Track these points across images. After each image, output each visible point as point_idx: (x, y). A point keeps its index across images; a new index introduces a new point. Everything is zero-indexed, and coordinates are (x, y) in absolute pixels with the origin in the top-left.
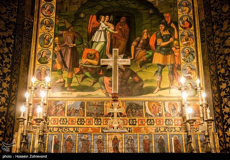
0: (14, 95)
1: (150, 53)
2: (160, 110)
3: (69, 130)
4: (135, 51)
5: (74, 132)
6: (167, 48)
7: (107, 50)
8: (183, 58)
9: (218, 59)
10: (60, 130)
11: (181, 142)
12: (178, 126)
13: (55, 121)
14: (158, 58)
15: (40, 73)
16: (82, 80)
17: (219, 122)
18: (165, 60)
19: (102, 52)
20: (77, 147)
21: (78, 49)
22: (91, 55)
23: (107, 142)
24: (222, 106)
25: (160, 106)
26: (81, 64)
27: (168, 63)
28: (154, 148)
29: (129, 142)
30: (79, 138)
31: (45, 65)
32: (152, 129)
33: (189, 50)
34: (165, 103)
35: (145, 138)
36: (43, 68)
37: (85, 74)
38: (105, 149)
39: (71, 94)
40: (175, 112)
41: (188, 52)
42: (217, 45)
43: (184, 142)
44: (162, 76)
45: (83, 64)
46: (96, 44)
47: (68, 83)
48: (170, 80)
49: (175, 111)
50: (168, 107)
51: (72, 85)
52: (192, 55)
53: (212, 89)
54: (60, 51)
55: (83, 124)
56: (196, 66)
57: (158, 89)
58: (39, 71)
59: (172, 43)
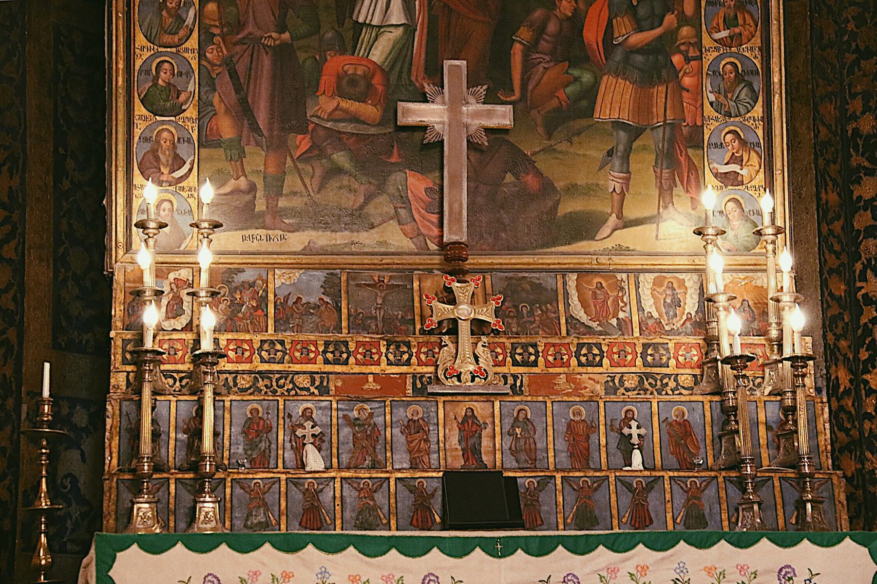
1: (587, 77)
2: (621, 304)
3: (294, 384)
4: (528, 67)
5: (312, 389)
6: (651, 57)
7: (415, 61)
8: (712, 98)
9: (851, 72)
11: (698, 431)
13: (240, 351)
14: (615, 100)
15: (154, 152)
16: (321, 187)
17: (838, 339)
18: (642, 106)
19: (397, 68)
20: (335, 445)
21: (302, 56)
22: (353, 82)
23: (441, 428)
25: (622, 289)
26: (317, 117)
27: (653, 119)
28: (604, 449)
29: (518, 431)
30: (341, 414)
31: (173, 118)
32: (593, 380)
33: (739, 66)
34: (642, 277)
35: (574, 415)
36: (165, 134)
38: (435, 452)
40: (676, 316)
41: (732, 75)
42: (853, 11)
43: (708, 429)
44: (628, 172)
45: (323, 119)
46: (373, 35)
48: (661, 188)
49: (678, 311)
51: (282, 203)
52: (750, 85)
54: (228, 63)
55: (346, 363)
56: (760, 132)
57: (613, 220)
58: (147, 147)
59: (671, 35)
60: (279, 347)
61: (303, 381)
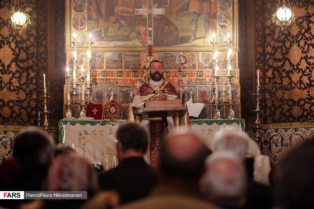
0: (43, 35)
2: (194, 60)
5: (114, 83)
8: (219, 5)
10: (102, 82)
12: (208, 78)
15: (76, 22)
16: (118, 30)
17: (259, 63)
18: (201, 9)
24: (265, 45)
25: (194, 56)
31: (81, 13)
36: (79, 17)
37: (121, 23)
39: (108, 43)
44: (197, 25)
47: (105, 33)
50: (202, 58)
51: (108, 34)
53: (255, 28)
55: (122, 76)
56: (231, 15)
57: (193, 38)
58: (75, 21)
60: (106, 73)
61: (112, 81)
